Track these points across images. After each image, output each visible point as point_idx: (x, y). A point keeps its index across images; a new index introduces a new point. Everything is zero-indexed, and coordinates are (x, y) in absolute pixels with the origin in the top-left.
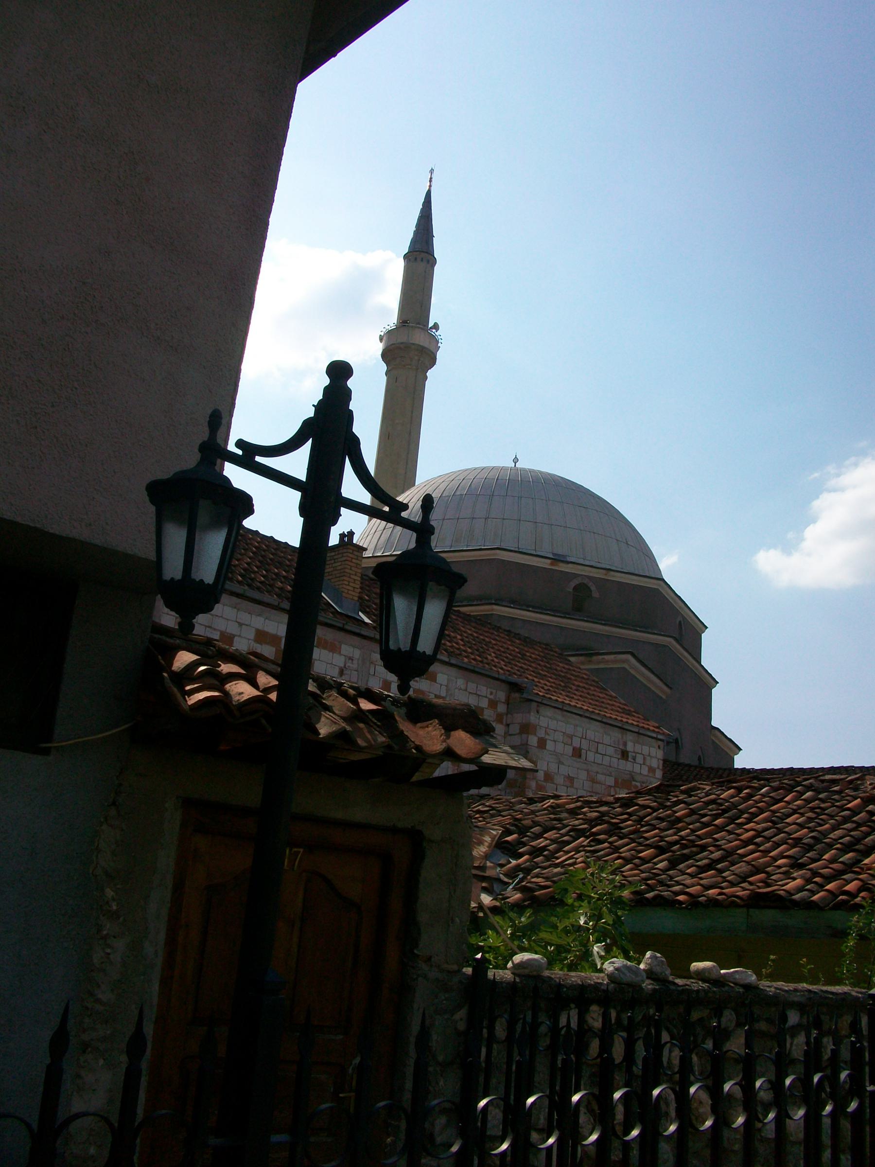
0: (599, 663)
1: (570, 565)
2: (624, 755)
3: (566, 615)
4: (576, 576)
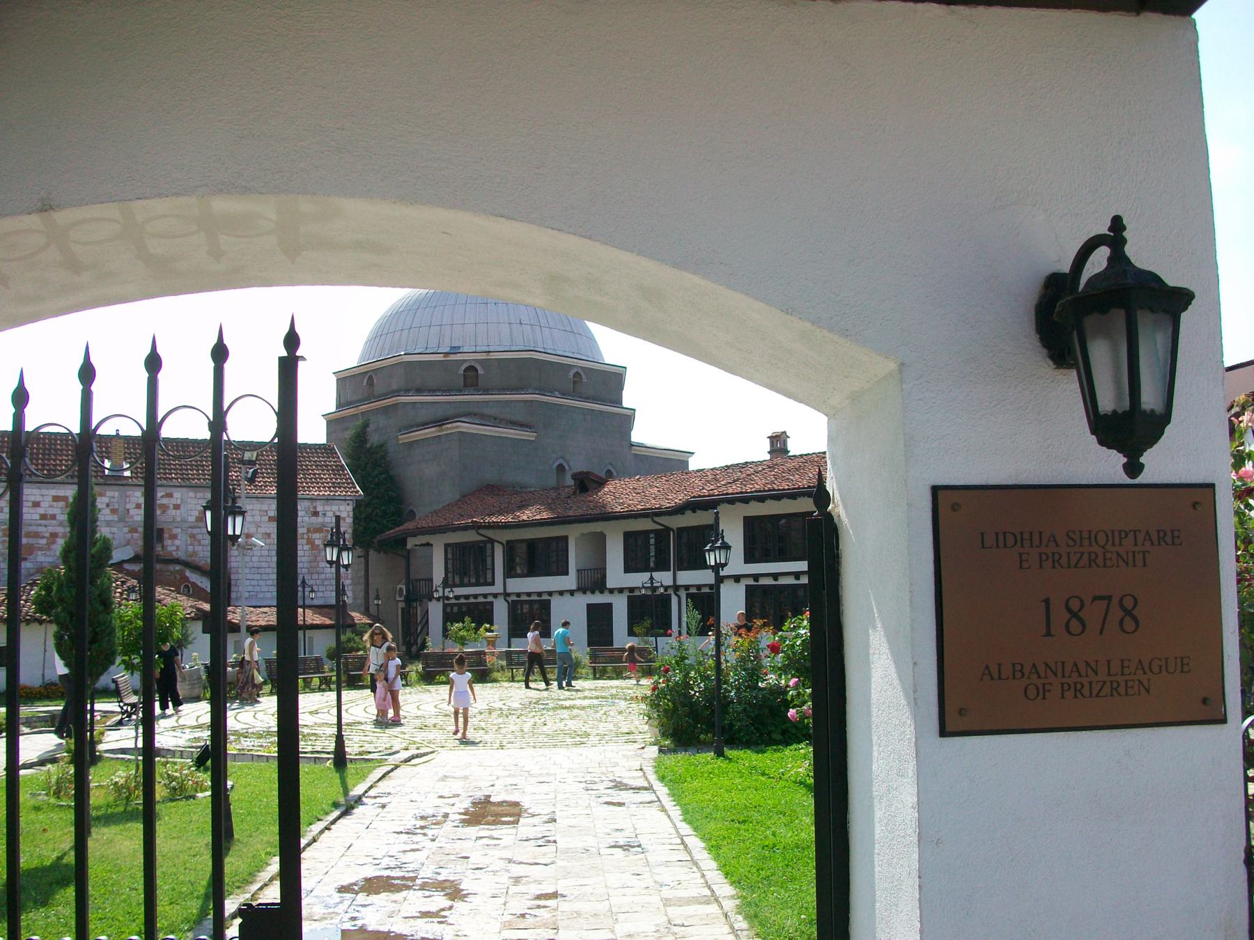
0: (448, 429)
1: (459, 355)
2: (316, 514)
3: (459, 391)
4: (464, 361)
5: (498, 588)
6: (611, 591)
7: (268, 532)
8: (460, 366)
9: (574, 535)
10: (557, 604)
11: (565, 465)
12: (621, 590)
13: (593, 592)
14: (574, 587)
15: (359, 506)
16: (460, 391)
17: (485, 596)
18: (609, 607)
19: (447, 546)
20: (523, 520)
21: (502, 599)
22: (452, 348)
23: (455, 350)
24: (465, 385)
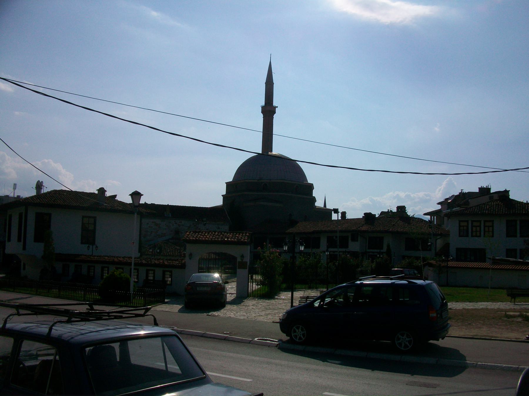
2: (219, 228)
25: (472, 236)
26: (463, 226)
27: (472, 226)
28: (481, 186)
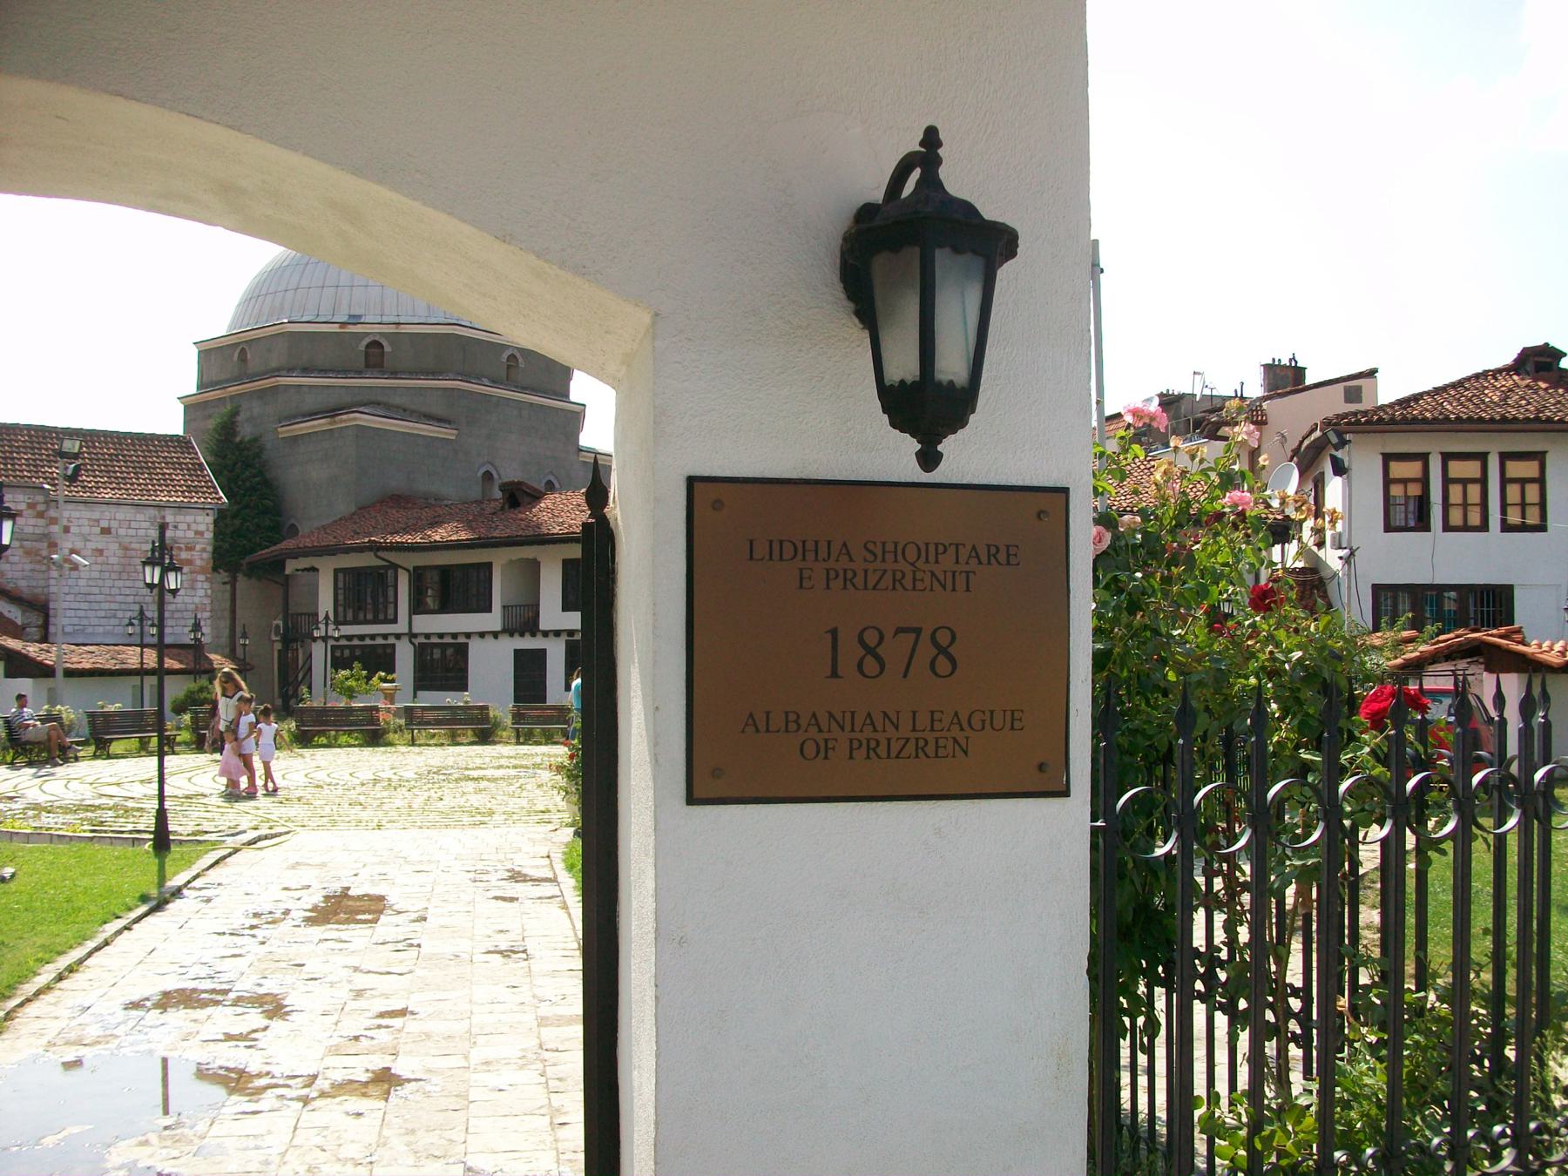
0: (341, 421)
3: (359, 373)
4: (367, 334)
5: (401, 627)
6: (546, 634)
7: (100, 547)
8: (361, 340)
9: (500, 559)
10: (476, 648)
11: (494, 473)
12: (557, 633)
13: (522, 635)
14: (498, 628)
15: (221, 517)
16: (360, 372)
17: (385, 636)
18: (541, 655)
19: (336, 571)
20: (435, 541)
21: (405, 640)
22: (350, 316)
23: (355, 320)
24: (367, 366)
25: (1447, 528)
26: (1404, 482)
27: (1447, 481)
28: (1274, 360)
